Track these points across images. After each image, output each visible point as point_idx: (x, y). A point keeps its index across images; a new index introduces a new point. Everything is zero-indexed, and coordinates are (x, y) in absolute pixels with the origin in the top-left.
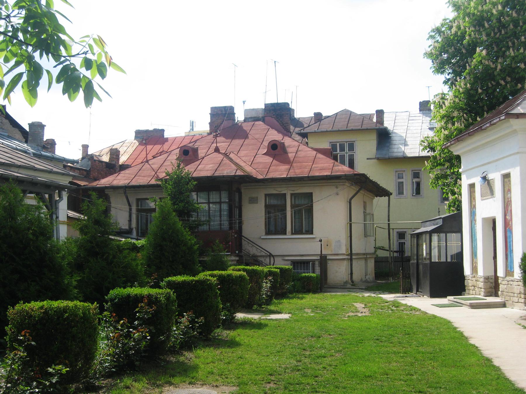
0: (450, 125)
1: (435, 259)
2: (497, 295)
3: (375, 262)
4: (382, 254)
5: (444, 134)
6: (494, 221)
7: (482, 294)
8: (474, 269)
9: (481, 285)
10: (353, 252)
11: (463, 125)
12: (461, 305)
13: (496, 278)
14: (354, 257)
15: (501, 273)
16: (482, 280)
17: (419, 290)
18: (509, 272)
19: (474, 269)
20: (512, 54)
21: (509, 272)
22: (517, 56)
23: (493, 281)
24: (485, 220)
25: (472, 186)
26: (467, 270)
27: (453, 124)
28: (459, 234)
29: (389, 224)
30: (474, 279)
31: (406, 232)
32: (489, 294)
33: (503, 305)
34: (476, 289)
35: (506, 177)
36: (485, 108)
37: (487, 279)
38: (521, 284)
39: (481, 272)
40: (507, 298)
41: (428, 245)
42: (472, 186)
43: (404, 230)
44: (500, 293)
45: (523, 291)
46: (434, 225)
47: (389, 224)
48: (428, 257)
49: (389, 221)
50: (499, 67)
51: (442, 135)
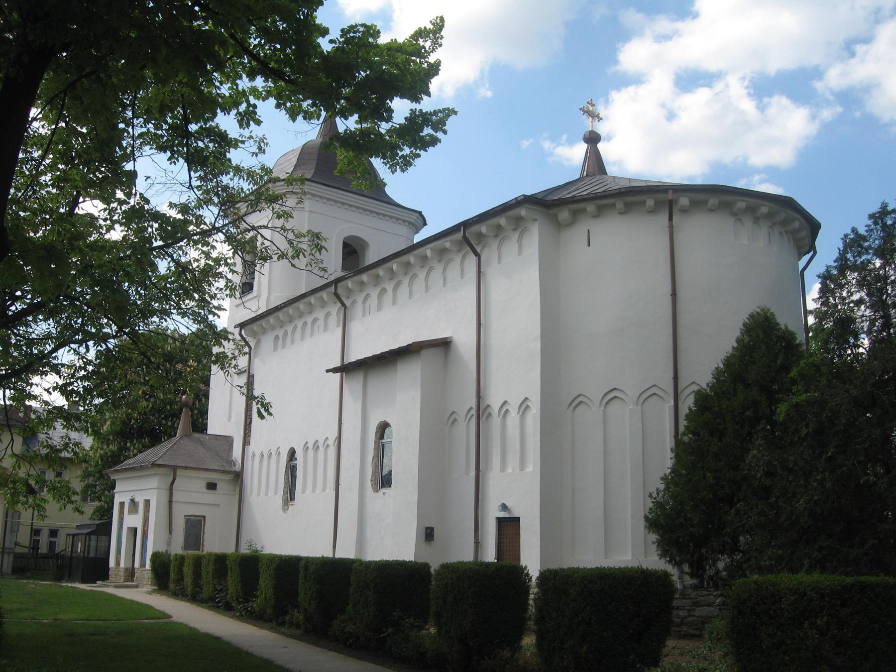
0: (105, 447)
1: (92, 555)
2: (132, 581)
3: (14, 557)
4: (18, 550)
5: (100, 453)
6: (135, 530)
7: (122, 580)
8: (118, 563)
9: (122, 574)
10: (6, 546)
11: (116, 447)
12: (108, 586)
13: (133, 568)
14: (5, 551)
15: (137, 565)
16: (123, 570)
17: (71, 579)
18: (143, 564)
19: (118, 563)
20: (162, 397)
21: (143, 564)
22: (166, 399)
23: (130, 571)
24: (129, 528)
25: (122, 504)
26: (112, 563)
27: (108, 445)
28: (108, 537)
29: (32, 523)
30: (117, 570)
31: (41, 529)
32: (126, 580)
33: (137, 587)
34: (118, 577)
35: (147, 502)
36: (136, 435)
37: (126, 569)
38: (150, 572)
39: (122, 565)
40: (140, 582)
41: (83, 543)
42: (122, 504)
43: (41, 528)
44: (135, 579)
45: (150, 577)
46: (88, 528)
47: (32, 523)
48: (82, 554)
49: (32, 520)
50: (151, 405)
51: (98, 455)
